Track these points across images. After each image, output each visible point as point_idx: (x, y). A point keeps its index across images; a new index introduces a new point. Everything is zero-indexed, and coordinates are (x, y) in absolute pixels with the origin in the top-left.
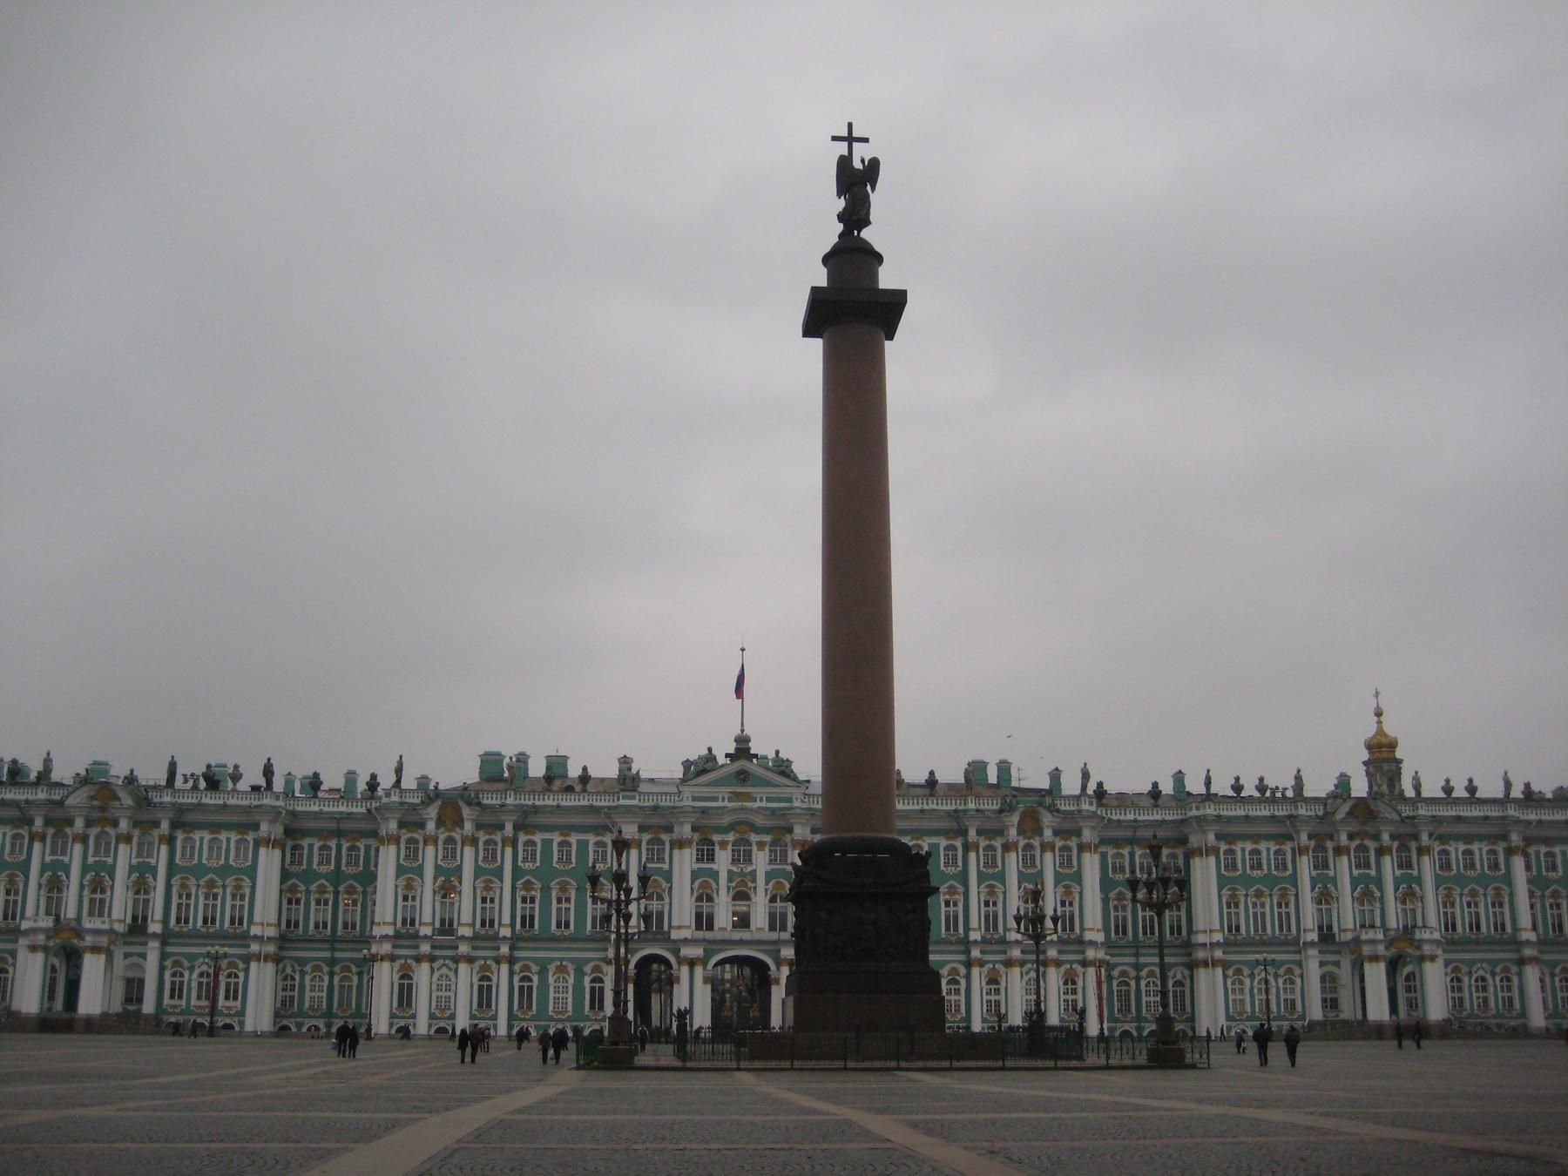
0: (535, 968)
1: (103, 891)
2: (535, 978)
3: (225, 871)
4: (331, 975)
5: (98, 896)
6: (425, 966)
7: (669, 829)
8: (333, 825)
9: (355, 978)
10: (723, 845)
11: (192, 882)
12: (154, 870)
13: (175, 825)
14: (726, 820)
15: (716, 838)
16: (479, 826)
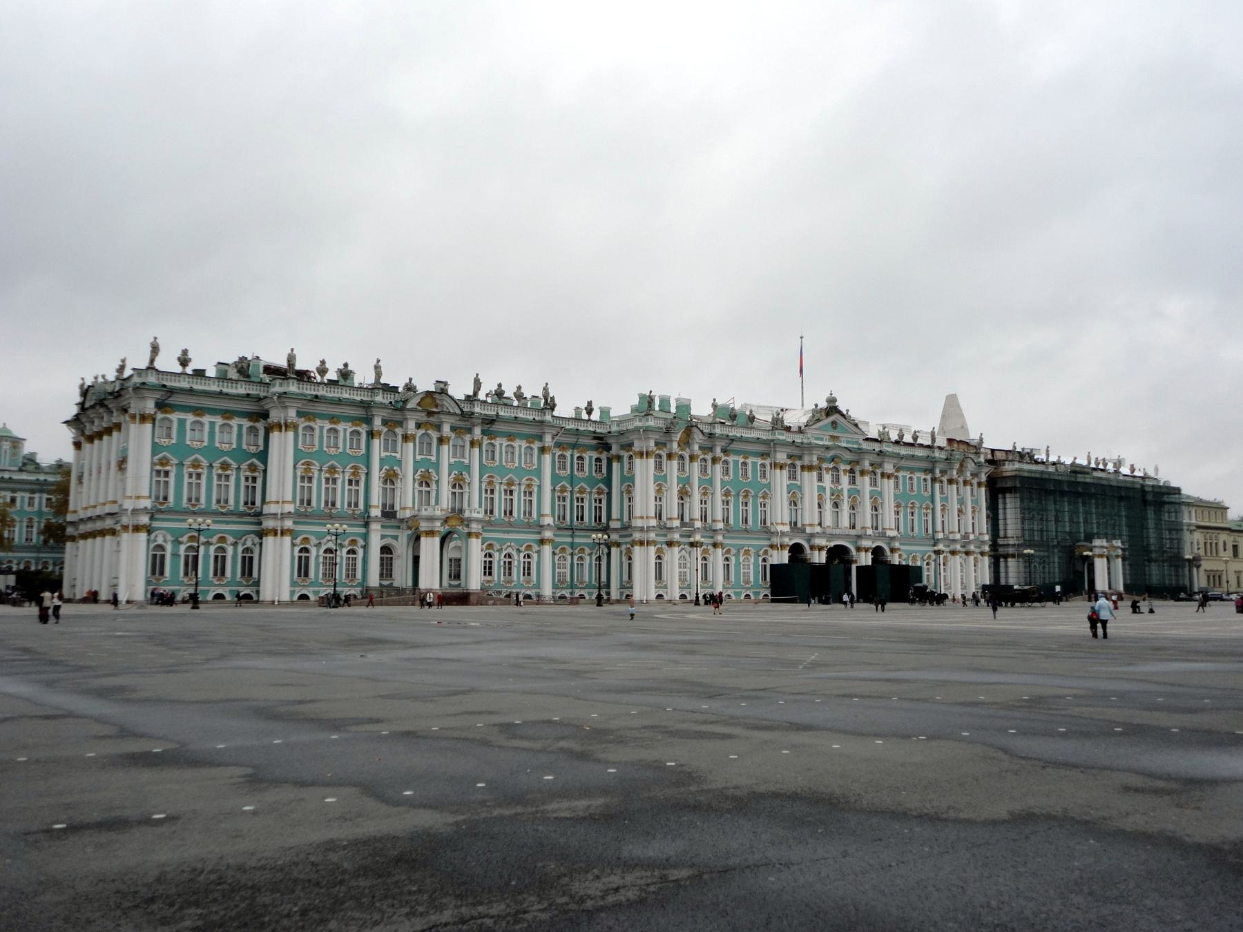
0: (733, 551)
1: (428, 485)
2: (733, 558)
3: (520, 471)
4: (572, 555)
5: (424, 489)
6: (676, 549)
7: (800, 458)
8: (572, 440)
9: (588, 558)
10: (827, 470)
11: (497, 480)
12: (468, 468)
13: (483, 432)
14: (831, 454)
15: (824, 466)
16: (700, 448)
